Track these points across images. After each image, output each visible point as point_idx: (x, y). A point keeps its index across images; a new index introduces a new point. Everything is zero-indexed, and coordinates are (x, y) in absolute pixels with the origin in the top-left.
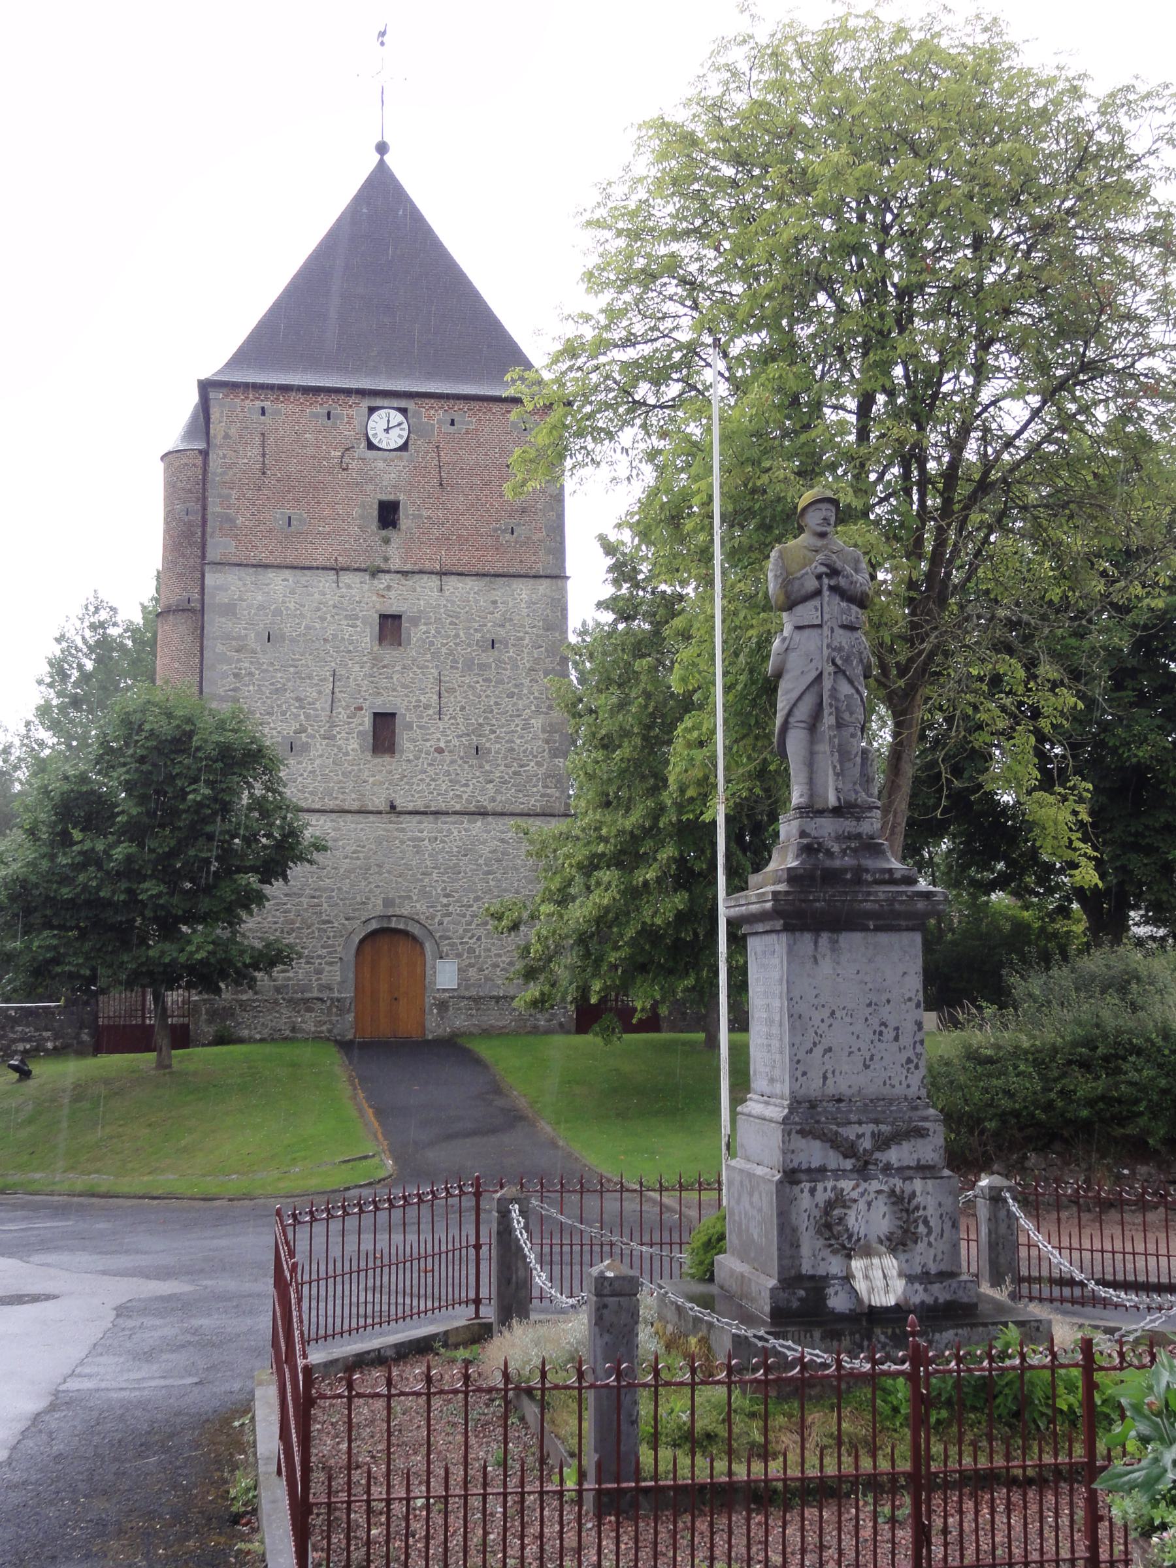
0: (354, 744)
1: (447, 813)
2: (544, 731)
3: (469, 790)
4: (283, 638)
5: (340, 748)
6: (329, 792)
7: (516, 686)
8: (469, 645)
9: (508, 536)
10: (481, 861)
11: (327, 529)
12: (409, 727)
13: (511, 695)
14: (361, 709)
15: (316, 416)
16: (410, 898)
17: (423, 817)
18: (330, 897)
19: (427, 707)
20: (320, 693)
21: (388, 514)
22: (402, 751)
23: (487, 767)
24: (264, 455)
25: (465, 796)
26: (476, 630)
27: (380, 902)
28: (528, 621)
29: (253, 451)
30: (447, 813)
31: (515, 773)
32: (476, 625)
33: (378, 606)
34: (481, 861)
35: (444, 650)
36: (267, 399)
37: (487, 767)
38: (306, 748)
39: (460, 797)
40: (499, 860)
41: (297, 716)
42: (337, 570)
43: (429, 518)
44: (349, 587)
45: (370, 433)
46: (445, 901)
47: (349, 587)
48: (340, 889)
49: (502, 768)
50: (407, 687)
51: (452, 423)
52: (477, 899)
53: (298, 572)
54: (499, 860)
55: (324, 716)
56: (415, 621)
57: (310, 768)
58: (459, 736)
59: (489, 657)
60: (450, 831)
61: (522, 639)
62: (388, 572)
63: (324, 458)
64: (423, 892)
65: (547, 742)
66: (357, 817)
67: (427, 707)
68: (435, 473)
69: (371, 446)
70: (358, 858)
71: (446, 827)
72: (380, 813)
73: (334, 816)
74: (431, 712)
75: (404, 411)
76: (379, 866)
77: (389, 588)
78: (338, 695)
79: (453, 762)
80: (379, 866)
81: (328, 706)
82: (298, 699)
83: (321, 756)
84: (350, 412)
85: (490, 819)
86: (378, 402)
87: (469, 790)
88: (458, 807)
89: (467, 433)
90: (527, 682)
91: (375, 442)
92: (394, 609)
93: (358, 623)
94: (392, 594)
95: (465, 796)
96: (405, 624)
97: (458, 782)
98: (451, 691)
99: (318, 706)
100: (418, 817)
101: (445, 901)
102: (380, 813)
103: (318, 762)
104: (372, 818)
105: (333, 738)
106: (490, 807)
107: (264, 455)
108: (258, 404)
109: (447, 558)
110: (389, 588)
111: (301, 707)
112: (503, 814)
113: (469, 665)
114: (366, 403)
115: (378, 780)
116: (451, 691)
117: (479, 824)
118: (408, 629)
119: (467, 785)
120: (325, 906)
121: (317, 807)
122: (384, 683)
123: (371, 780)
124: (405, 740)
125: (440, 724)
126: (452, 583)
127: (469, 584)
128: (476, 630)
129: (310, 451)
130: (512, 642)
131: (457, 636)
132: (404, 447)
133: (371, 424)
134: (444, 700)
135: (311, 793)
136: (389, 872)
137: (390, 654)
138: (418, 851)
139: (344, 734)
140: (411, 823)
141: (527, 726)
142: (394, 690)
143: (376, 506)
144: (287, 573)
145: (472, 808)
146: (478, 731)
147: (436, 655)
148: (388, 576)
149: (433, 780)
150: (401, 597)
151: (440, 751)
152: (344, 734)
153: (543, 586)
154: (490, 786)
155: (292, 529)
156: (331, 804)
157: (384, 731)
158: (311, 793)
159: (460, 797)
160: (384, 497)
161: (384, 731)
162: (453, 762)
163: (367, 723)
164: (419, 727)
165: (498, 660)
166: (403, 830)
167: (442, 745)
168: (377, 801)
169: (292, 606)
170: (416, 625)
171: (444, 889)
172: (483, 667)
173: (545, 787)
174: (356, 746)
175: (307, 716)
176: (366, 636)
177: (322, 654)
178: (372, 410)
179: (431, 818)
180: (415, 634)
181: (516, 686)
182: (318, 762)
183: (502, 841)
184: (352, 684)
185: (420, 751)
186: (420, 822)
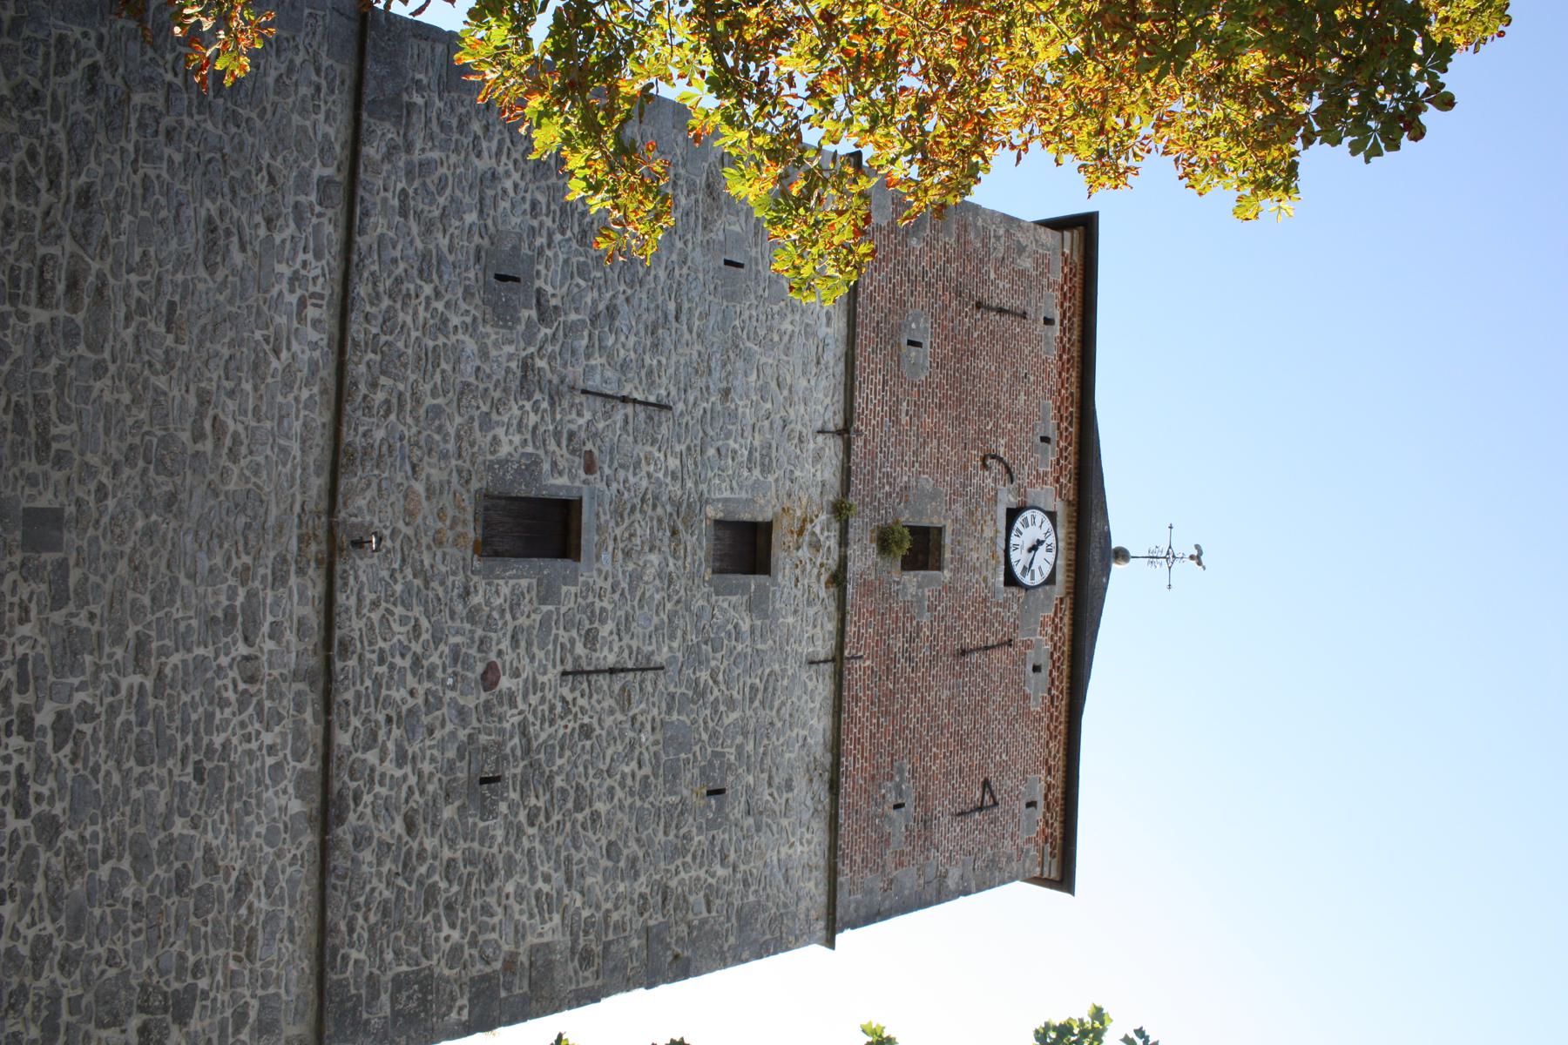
0: (509, 445)
1: (327, 709)
2: (534, 950)
3: (389, 767)
4: (731, 297)
5: (497, 406)
6: (389, 363)
7: (633, 861)
8: (714, 735)
9: (892, 799)
10: (179, 826)
11: (904, 419)
12: (548, 594)
13: (612, 850)
14: (590, 468)
15: (1045, 421)
16: (59, 600)
17: (316, 638)
18: (71, 336)
19: (591, 639)
20: (624, 367)
21: (922, 548)
22: (489, 575)
23: (448, 812)
24: (1001, 311)
25: (372, 757)
26: (740, 748)
27: (45, 501)
28: (755, 866)
29: (1001, 292)
30: (327, 709)
31: (432, 891)
32: (750, 747)
33: (785, 521)
34: (179, 826)
35: (704, 675)
36: (1063, 331)
37: (448, 812)
38: (504, 315)
39: (372, 740)
40: (181, 882)
41: (574, 300)
42: (845, 432)
43: (919, 628)
44: (818, 457)
45: (1028, 514)
46: (45, 718)
47: (818, 457)
48: (99, 370)
49: (447, 853)
50: (632, 589)
51: (1036, 669)
52: (49, 828)
53: (841, 349)
54: (181, 882)
55: (574, 372)
56: (758, 605)
57: (455, 320)
58: (523, 728)
59: (689, 789)
60: (271, 720)
61: (724, 858)
62: (843, 542)
63: (996, 425)
64: (71, 647)
65: (510, 963)
66: (320, 440)
67: (591, 639)
68: (977, 641)
69: (1013, 514)
70: (198, 436)
71: (287, 704)
72: (332, 510)
73: (327, 372)
74: (580, 649)
75: (1051, 580)
76: (172, 498)
77: (816, 546)
78: (621, 411)
79: (462, 713)
80: (172, 498)
81: (595, 383)
82: (612, 311)
83: (484, 354)
84: (1050, 479)
85: (309, 838)
86: (1062, 532)
87: (389, 767)
88: (343, 739)
89: (1026, 697)
90: (641, 885)
91: (1018, 525)
92: (781, 557)
93: (757, 472)
94: (805, 553)
95: (372, 757)
96: (753, 581)
97: (411, 733)
98: (625, 700)
99: (597, 361)
100: (315, 621)
101: (45, 718)
102: (332, 510)
103: (471, 346)
104: (318, 483)
105: (525, 390)
106: (344, 833)
107: (1001, 311)
108: (1057, 315)
109: (859, 670)
110: (816, 546)
111: (595, 318)
112: (324, 869)
113: (676, 740)
114: (1059, 507)
115: (416, 505)
116: (625, 700)
117: (296, 806)
118: (745, 589)
119: (401, 759)
120: (40, 316)
121: (356, 329)
122: (643, 531)
123: (419, 487)
124: (516, 580)
125: (553, 674)
126: (822, 687)
127: (819, 725)
128: (740, 748)
129: (1004, 399)
130: (721, 836)
131: (731, 704)
132: (1011, 580)
133: (1039, 516)
134: (603, 681)
135: (388, 317)
136: (150, 532)
137: (699, 544)
138: (218, 624)
139: (533, 419)
140: (299, 600)
141: (546, 905)
142: (627, 554)
143: (936, 522)
144: (840, 323)
145: (343, 781)
146: (535, 777)
147: (694, 656)
148: (833, 543)
149: (417, 662)
150: (798, 571)
151: (489, 678)
152: (533, 419)
153: (813, 888)
154: (399, 826)
155: (905, 347)
156: (358, 370)
157: (540, 528)
158: (388, 317)
159: (372, 740)
160: (948, 539)
161: (540, 528)
162: (462, 713)
163: (558, 484)
164: (545, 623)
165: (684, 808)
166: (279, 579)
167: (505, 683)
168: (361, 502)
169: (786, 326)
170: (750, 609)
171: (87, 713)
172: (673, 774)
173: (399, 983)
174: (504, 450)
175: (572, 329)
176: (732, 492)
177: (700, 382)
178: (1052, 516)
179: (313, 662)
180: (730, 606)
181: (633, 861)
182: (471, 346)
183: (243, 886)
184: (641, 450)
185: (489, 625)
186: (302, 629)
